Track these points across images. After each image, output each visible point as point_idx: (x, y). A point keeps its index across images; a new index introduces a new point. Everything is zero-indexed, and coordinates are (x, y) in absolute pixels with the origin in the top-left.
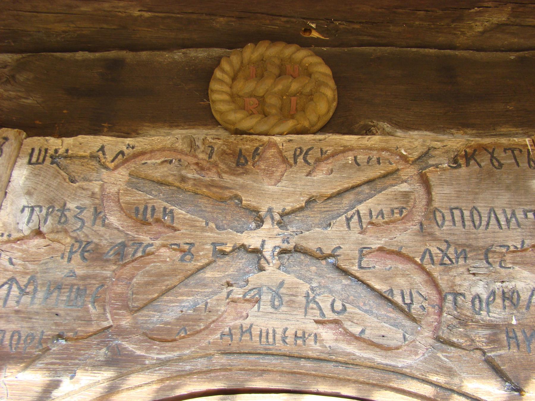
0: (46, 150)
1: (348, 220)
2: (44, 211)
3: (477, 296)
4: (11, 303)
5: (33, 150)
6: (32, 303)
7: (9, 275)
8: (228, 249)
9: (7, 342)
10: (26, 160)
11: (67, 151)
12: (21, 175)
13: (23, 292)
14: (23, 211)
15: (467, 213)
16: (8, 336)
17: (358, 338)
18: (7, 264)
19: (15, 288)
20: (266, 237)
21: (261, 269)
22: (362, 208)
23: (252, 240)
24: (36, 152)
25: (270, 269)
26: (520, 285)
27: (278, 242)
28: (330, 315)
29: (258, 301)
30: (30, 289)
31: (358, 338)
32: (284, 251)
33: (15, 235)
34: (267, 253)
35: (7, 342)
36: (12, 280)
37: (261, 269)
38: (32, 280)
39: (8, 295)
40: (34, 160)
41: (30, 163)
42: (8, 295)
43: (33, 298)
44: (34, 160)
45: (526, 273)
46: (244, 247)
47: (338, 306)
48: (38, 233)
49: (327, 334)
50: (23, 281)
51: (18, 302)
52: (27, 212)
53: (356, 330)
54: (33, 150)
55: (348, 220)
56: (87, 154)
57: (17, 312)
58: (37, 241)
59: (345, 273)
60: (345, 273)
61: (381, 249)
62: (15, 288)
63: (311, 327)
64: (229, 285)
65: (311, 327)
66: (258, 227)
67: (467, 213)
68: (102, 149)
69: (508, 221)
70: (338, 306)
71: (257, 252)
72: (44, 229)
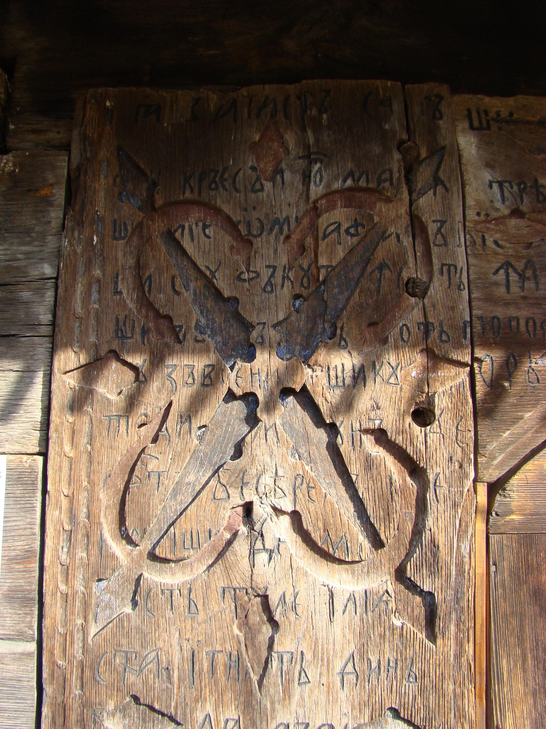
0: (486, 112)
2: (515, 188)
4: (515, 289)
5: (469, 111)
6: (537, 289)
7: (502, 259)
9: (523, 329)
10: (466, 125)
11: (511, 114)
12: (468, 144)
13: (522, 277)
14: (491, 187)
16: (522, 323)
18: (494, 246)
24: (474, 115)
30: (529, 273)
33: (494, 215)
35: (523, 329)
36: (507, 265)
38: (529, 264)
39: (508, 281)
40: (476, 124)
41: (472, 127)
42: (508, 281)
43: (537, 283)
44: (476, 124)
48: (516, 213)
50: (520, 265)
51: (522, 288)
52: (495, 186)
54: (469, 111)
56: (536, 119)
57: (524, 298)
58: (513, 222)
72: (524, 208)
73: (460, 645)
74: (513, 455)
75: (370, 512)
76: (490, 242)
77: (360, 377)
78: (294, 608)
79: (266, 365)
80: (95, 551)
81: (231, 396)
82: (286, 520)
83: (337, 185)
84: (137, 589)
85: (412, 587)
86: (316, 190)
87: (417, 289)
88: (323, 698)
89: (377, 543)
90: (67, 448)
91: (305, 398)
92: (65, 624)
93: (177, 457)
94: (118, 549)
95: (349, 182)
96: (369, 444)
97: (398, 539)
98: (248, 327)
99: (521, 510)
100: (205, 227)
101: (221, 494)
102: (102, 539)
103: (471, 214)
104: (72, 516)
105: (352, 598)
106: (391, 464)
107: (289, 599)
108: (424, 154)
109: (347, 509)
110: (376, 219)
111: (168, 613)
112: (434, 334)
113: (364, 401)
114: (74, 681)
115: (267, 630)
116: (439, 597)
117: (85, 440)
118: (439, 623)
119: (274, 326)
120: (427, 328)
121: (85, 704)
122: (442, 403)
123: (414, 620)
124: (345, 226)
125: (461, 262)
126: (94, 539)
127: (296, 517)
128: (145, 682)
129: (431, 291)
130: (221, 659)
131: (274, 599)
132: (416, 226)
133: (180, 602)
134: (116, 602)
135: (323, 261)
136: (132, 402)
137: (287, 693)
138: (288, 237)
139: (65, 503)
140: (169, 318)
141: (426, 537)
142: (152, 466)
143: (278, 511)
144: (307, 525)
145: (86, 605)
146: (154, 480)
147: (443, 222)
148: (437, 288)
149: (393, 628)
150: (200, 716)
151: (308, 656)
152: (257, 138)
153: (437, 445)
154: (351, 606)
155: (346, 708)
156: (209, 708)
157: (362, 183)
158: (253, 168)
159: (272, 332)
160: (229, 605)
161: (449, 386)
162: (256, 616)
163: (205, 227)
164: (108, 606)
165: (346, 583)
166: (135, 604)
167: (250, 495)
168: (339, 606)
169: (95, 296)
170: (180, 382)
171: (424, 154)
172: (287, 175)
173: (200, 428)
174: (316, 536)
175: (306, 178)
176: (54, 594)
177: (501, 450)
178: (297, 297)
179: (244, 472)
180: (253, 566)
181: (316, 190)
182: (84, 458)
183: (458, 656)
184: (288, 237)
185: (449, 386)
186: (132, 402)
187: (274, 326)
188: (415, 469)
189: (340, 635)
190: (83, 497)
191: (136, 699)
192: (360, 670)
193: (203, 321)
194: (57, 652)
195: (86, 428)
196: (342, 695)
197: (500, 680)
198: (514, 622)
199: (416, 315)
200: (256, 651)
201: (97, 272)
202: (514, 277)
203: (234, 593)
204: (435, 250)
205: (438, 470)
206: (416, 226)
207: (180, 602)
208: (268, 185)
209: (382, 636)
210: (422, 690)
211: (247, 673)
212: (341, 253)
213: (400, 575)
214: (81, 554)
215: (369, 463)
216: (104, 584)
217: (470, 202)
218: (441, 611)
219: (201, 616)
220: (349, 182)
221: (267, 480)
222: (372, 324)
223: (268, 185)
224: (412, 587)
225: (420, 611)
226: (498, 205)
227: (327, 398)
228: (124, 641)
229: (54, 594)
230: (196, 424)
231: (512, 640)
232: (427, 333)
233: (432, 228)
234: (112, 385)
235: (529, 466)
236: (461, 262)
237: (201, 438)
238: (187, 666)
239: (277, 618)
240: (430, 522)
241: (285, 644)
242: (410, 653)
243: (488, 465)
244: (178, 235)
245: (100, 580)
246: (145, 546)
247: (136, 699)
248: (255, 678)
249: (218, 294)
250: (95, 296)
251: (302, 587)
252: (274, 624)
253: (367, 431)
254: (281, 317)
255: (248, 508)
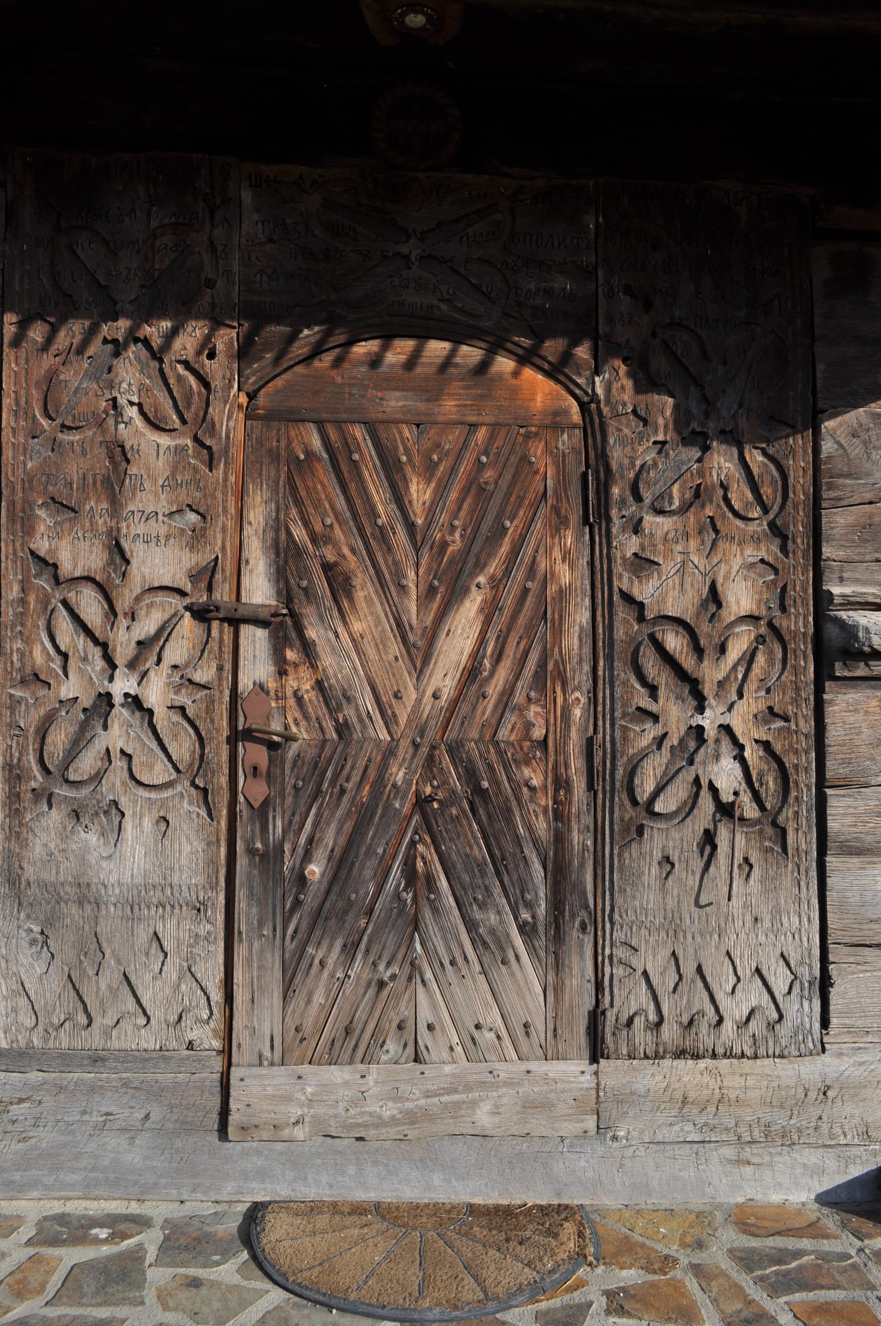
1: (461, 238)
3: (530, 290)
8: (390, 254)
12: (247, 197)
15: (534, 237)
17: (460, 310)
19: (265, 277)
20: (411, 248)
21: (410, 268)
22: (470, 231)
23: (404, 250)
25: (414, 268)
26: (556, 285)
27: (419, 251)
28: (446, 296)
29: (407, 287)
31: (460, 310)
32: (422, 257)
34: (413, 259)
37: (410, 268)
41: (251, 185)
45: (561, 278)
46: (399, 254)
47: (451, 291)
48: (271, 240)
49: (444, 307)
52: (260, 224)
53: (460, 305)
55: (461, 238)
59: (456, 272)
60: (456, 272)
61: (478, 259)
62: (265, 277)
63: (436, 302)
64: (391, 276)
65: (436, 302)
66: (407, 241)
67: (534, 237)
68: (301, 177)
69: (559, 244)
70: (451, 291)
71: (407, 258)
72: (275, 238)
73: (226, 474)
74: (261, 378)
75: (179, 404)
76: (253, 257)
77: (174, 332)
78: (138, 451)
79: (123, 324)
80: (30, 421)
81: (105, 341)
82: (135, 408)
83: (166, 221)
84: (54, 445)
85: (202, 444)
86: (154, 223)
87: (210, 284)
88: (152, 498)
89: (184, 421)
90: (13, 366)
91: (146, 342)
92: (14, 459)
93: (76, 373)
94: (44, 423)
95: (173, 220)
96: (180, 368)
97: (195, 419)
98: (115, 303)
99: (263, 408)
100: (90, 243)
101: (100, 393)
102: (34, 416)
103: (243, 240)
104: (17, 403)
105: (169, 448)
106: (192, 381)
107: (135, 447)
108: (218, 202)
109: (168, 404)
110: (188, 242)
111: (71, 455)
112: (218, 309)
113: (177, 344)
114: (19, 488)
115: (124, 464)
116: (215, 448)
117: (23, 362)
118: (215, 463)
119: (130, 303)
120: (213, 305)
121: (25, 501)
122: (220, 347)
123: (203, 462)
124: (170, 246)
125: (236, 268)
126: (30, 415)
127: (140, 405)
128: (59, 491)
129: (217, 286)
130: (99, 477)
131: (128, 447)
132: (212, 246)
133: (77, 448)
134: (42, 450)
135: (157, 266)
136: (49, 340)
137: (134, 494)
138: (138, 251)
139: (13, 395)
140: (70, 296)
141: (209, 417)
142: (62, 377)
143: (132, 404)
144: (146, 409)
145: (25, 449)
146: (63, 384)
147: (226, 245)
148: (220, 284)
149: (190, 463)
150: (88, 508)
151: (145, 477)
152: (121, 188)
153: (214, 369)
154: (168, 452)
155: (164, 503)
156: (93, 503)
157: (181, 220)
158: (118, 208)
159: (128, 306)
160: (103, 451)
161: (226, 338)
162: (119, 458)
163: (90, 243)
164: (39, 452)
165: (165, 441)
166: (53, 450)
167: (115, 393)
168: (161, 453)
169: (26, 281)
170: (77, 332)
171: (218, 202)
172: (138, 213)
173: (89, 358)
174: (151, 416)
175: (149, 215)
176: (7, 443)
177: (253, 375)
178: (143, 287)
179: (112, 381)
180: (116, 430)
181: (154, 223)
182: (23, 372)
183: (226, 480)
184: (138, 251)
185: (226, 338)
186: (49, 340)
187: (130, 303)
188: (205, 384)
189: (161, 466)
190: (23, 392)
191: (53, 499)
192: (172, 484)
193: (91, 299)
194: (10, 473)
195: (24, 355)
196: (163, 497)
197: (248, 495)
198: (258, 466)
199: (207, 299)
200: (118, 475)
201: (28, 267)
202: (265, 278)
203: (106, 443)
204: (221, 261)
205: (217, 383)
206: (212, 246)
207: (77, 448)
208: (127, 219)
209: (184, 468)
210: (205, 496)
211: (112, 485)
212: (167, 262)
213: (196, 439)
214: (22, 423)
215: (179, 378)
216: (36, 440)
217: (243, 233)
218: (216, 456)
219: (88, 457)
220: (173, 220)
221: (124, 385)
222: (184, 303)
223: (127, 219)
224: (202, 444)
225: (206, 457)
226: (260, 235)
227: (157, 342)
228: (47, 469)
229: (7, 443)
230: (87, 355)
231: (256, 475)
232: (213, 309)
233: (220, 248)
234: (37, 333)
235: (270, 385)
236: (236, 268)
237: (90, 364)
238: (81, 482)
239: (129, 456)
240: (211, 410)
241: (133, 470)
242: (198, 476)
243: (246, 382)
244: (74, 247)
245: (34, 437)
246: (59, 421)
247: (53, 499)
248: (117, 489)
249: (99, 283)
250: (26, 281)
251: (142, 442)
252: (128, 461)
253: (179, 362)
254: (133, 297)
255: (114, 400)
